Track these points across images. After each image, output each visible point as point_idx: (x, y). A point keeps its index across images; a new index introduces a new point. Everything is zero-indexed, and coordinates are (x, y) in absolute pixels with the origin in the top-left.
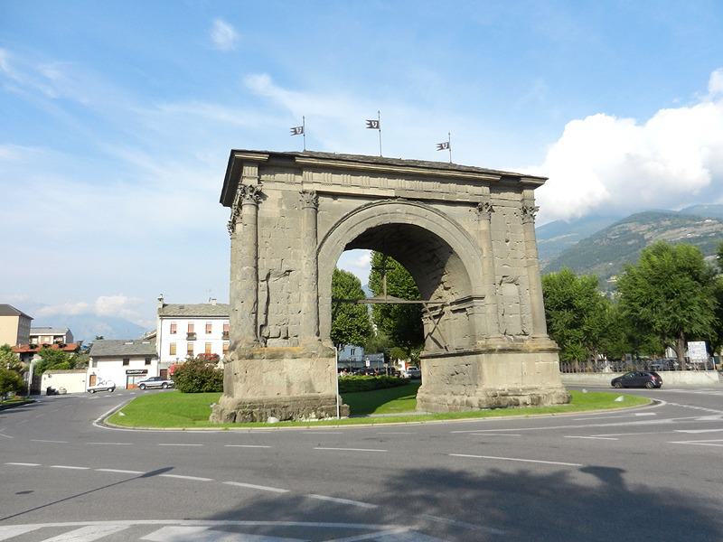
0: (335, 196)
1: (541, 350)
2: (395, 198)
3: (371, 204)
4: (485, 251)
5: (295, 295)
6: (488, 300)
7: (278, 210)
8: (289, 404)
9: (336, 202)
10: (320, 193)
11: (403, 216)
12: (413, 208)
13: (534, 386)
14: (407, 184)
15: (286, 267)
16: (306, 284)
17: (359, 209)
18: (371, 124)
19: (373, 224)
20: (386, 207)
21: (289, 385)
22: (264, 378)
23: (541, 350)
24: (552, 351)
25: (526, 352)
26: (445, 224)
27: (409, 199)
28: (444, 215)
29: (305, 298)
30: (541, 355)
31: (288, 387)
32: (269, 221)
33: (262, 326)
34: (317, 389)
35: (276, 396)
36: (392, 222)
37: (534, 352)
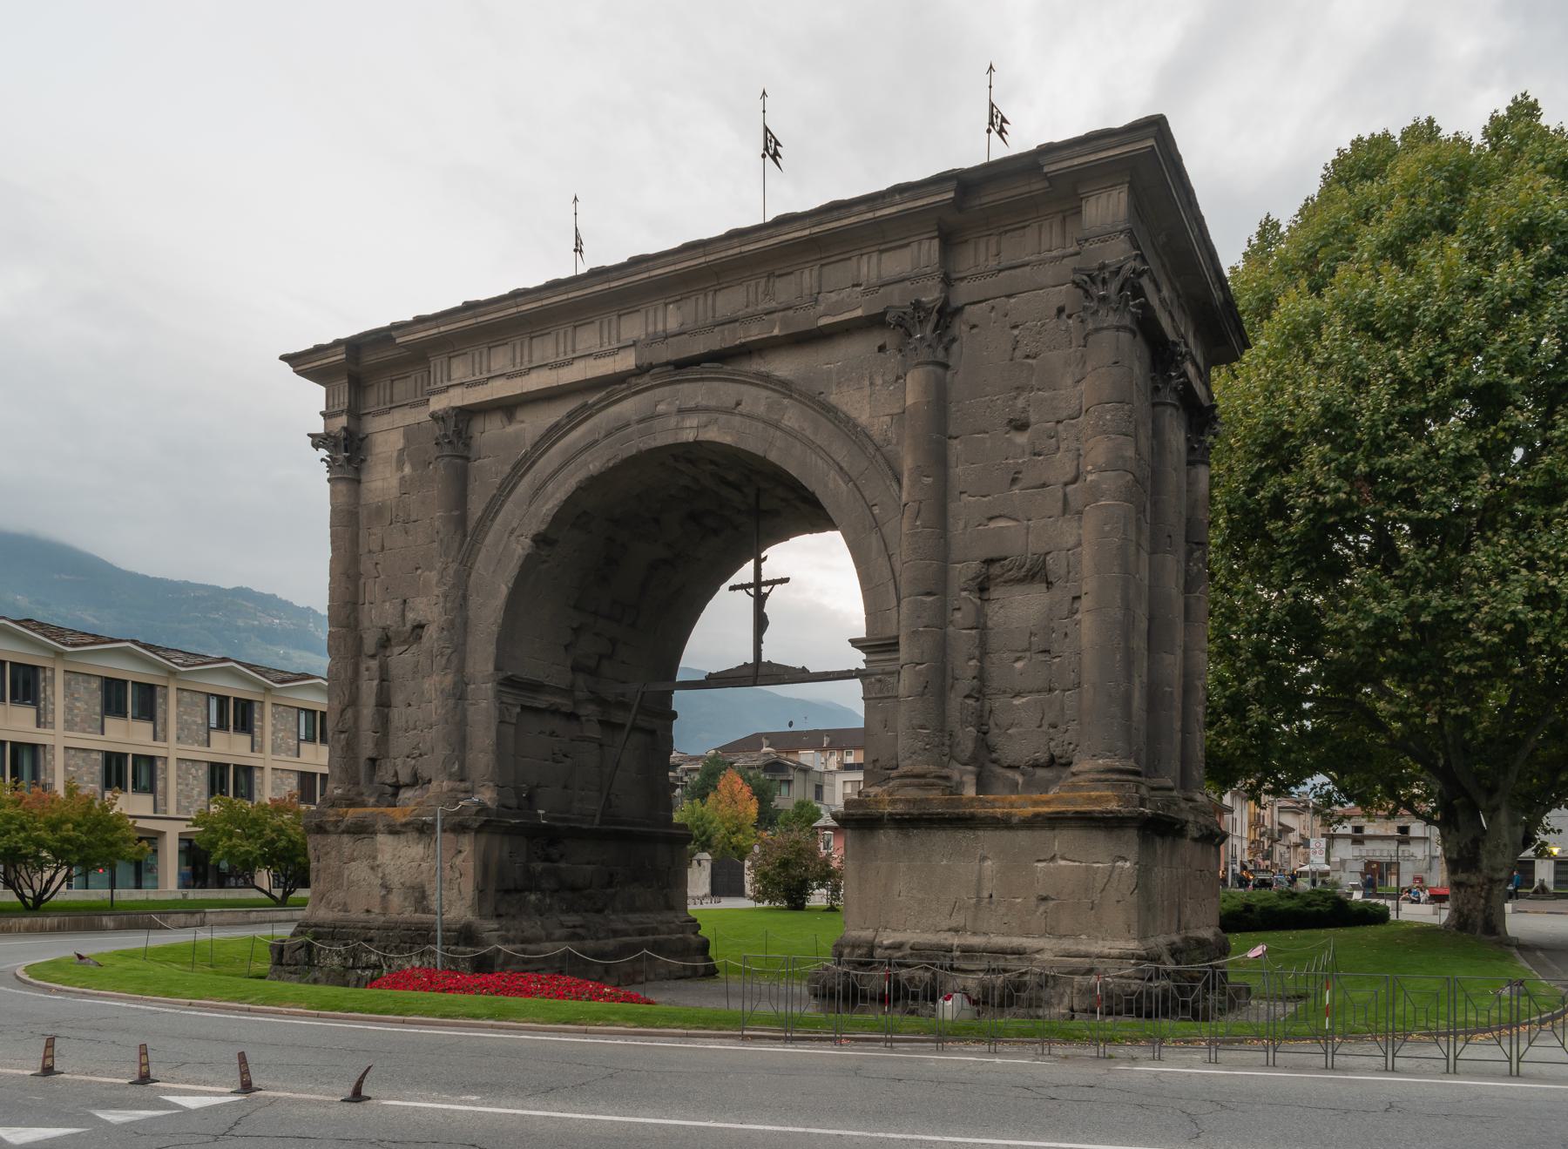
0: (508, 408)
1: (1054, 821)
2: (640, 371)
3: (585, 406)
4: (906, 481)
7: (394, 482)
9: (511, 429)
10: (467, 414)
11: (673, 422)
12: (695, 392)
17: (554, 433)
19: (594, 464)
20: (628, 408)
23: (1054, 821)
26: (793, 417)
27: (682, 365)
28: (785, 387)
30: (1060, 840)
32: (379, 511)
36: (644, 447)
37: (1031, 823)
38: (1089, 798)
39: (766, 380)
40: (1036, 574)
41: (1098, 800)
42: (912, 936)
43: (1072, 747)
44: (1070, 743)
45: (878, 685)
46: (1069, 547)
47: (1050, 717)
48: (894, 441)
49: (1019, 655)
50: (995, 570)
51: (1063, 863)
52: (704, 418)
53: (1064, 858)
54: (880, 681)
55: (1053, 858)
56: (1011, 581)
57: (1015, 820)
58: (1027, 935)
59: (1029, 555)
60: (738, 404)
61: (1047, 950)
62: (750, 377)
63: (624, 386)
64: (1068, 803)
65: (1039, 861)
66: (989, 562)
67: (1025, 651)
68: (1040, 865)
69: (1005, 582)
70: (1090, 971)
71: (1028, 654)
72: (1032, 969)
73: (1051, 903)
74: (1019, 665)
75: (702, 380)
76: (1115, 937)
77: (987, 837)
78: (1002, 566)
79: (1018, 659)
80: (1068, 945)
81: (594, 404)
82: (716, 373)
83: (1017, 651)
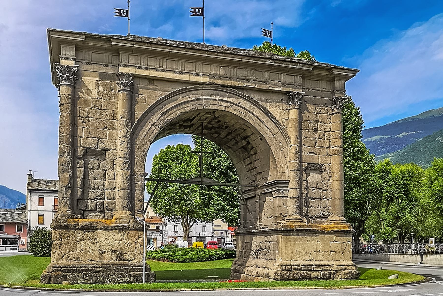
4: (292, 139)
5: (110, 173)
6: (292, 185)
8: (100, 269)
11: (217, 102)
13: (327, 263)
14: (222, 72)
15: (101, 146)
16: (119, 162)
17: (174, 94)
18: (195, 12)
20: (200, 94)
21: (102, 252)
22: (79, 245)
24: (345, 233)
25: (323, 233)
29: (119, 178)
31: (100, 254)
33: (78, 200)
34: (127, 256)
35: (90, 263)
37: (329, 233)
38: (342, 227)
39: (250, 100)
40: (319, 169)
41: (343, 227)
42: (301, 263)
43: (329, 213)
44: (329, 212)
45: (282, 193)
46: (328, 163)
47: (325, 205)
48: (286, 126)
49: (314, 189)
50: (310, 166)
51: (336, 242)
52: (228, 104)
53: (336, 241)
54: (282, 192)
55: (334, 242)
56: (312, 169)
57: (326, 232)
58: (328, 261)
59: (319, 164)
60: (239, 103)
61: (335, 264)
62: (245, 97)
63: (201, 86)
64: (337, 228)
65: (330, 242)
66: (309, 164)
67: (315, 188)
68: (331, 243)
69: (310, 169)
70: (345, 269)
71: (316, 189)
72: (332, 270)
73: (333, 253)
74: (313, 191)
75: (228, 92)
76: (348, 261)
77: (321, 236)
78: (311, 165)
79: (313, 190)
80: (338, 263)
81: (189, 89)
82: (234, 92)
83: (313, 188)
